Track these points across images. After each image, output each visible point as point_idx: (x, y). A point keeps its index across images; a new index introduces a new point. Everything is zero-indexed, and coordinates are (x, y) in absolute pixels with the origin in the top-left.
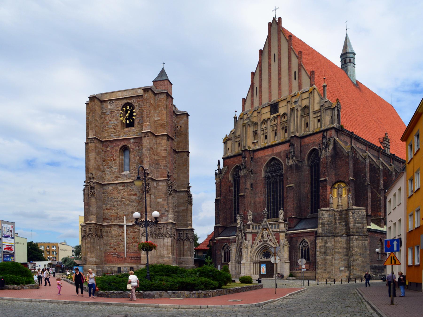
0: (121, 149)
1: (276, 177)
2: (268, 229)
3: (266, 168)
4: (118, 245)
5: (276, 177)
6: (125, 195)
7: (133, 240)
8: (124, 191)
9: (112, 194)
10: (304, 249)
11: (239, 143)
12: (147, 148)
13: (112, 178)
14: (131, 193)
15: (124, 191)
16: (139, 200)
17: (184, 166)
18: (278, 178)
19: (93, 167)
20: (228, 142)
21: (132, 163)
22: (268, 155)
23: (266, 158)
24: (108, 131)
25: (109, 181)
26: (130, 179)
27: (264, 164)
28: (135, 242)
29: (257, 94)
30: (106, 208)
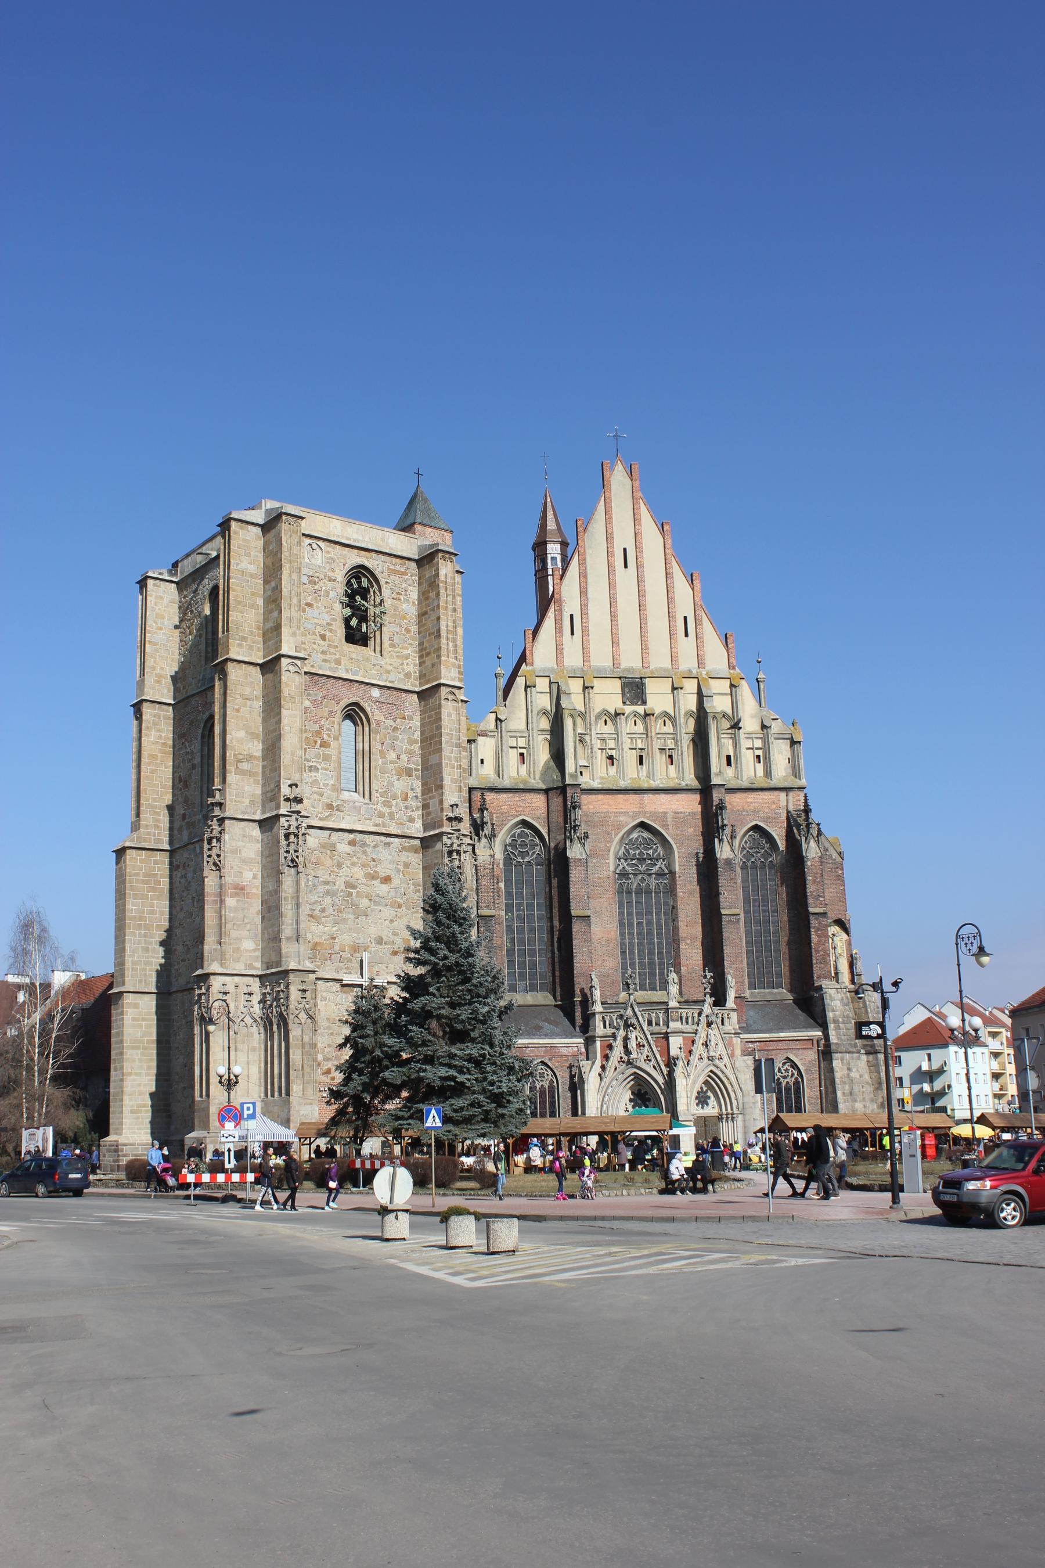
1: (645, 877)
3: (618, 847)
5: (645, 877)
11: (522, 754)
13: (314, 807)
14: (375, 871)
15: (355, 859)
16: (399, 900)
18: (653, 882)
20: (481, 740)
22: (626, 813)
23: (622, 819)
26: (371, 823)
27: (616, 835)
29: (572, 633)
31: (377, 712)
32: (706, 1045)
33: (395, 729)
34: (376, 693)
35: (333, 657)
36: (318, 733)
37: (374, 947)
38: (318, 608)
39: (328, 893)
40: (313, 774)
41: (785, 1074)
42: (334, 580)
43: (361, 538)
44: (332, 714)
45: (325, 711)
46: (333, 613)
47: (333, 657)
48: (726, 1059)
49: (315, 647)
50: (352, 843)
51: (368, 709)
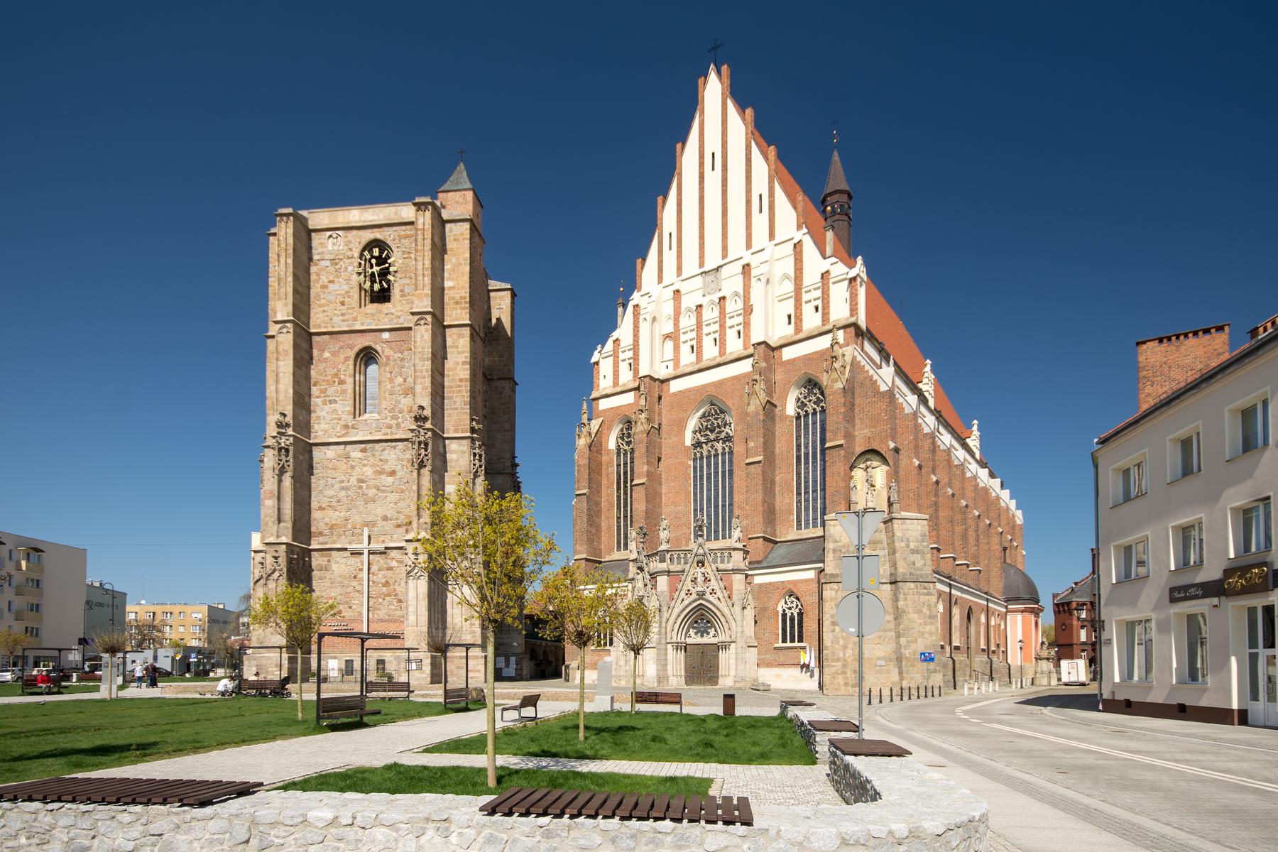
0: (357, 355)
2: (706, 564)
4: (347, 603)
6: (366, 474)
7: (384, 589)
8: (366, 462)
9: (334, 469)
10: (789, 615)
12: (424, 355)
15: (366, 462)
17: (504, 413)
19: (286, 397)
21: (385, 392)
24: (326, 308)
25: (328, 437)
26: (381, 433)
28: (389, 595)
30: (318, 505)
31: (387, 350)
32: (694, 581)
33: (403, 359)
34: (386, 335)
35: (351, 316)
36: (336, 375)
37: (380, 523)
38: (339, 282)
39: (343, 488)
40: (333, 405)
41: (790, 605)
42: (352, 258)
43: (376, 218)
44: (347, 359)
45: (342, 357)
46: (351, 282)
47: (351, 316)
48: (719, 594)
49: (335, 312)
50: (364, 451)
51: (378, 348)
